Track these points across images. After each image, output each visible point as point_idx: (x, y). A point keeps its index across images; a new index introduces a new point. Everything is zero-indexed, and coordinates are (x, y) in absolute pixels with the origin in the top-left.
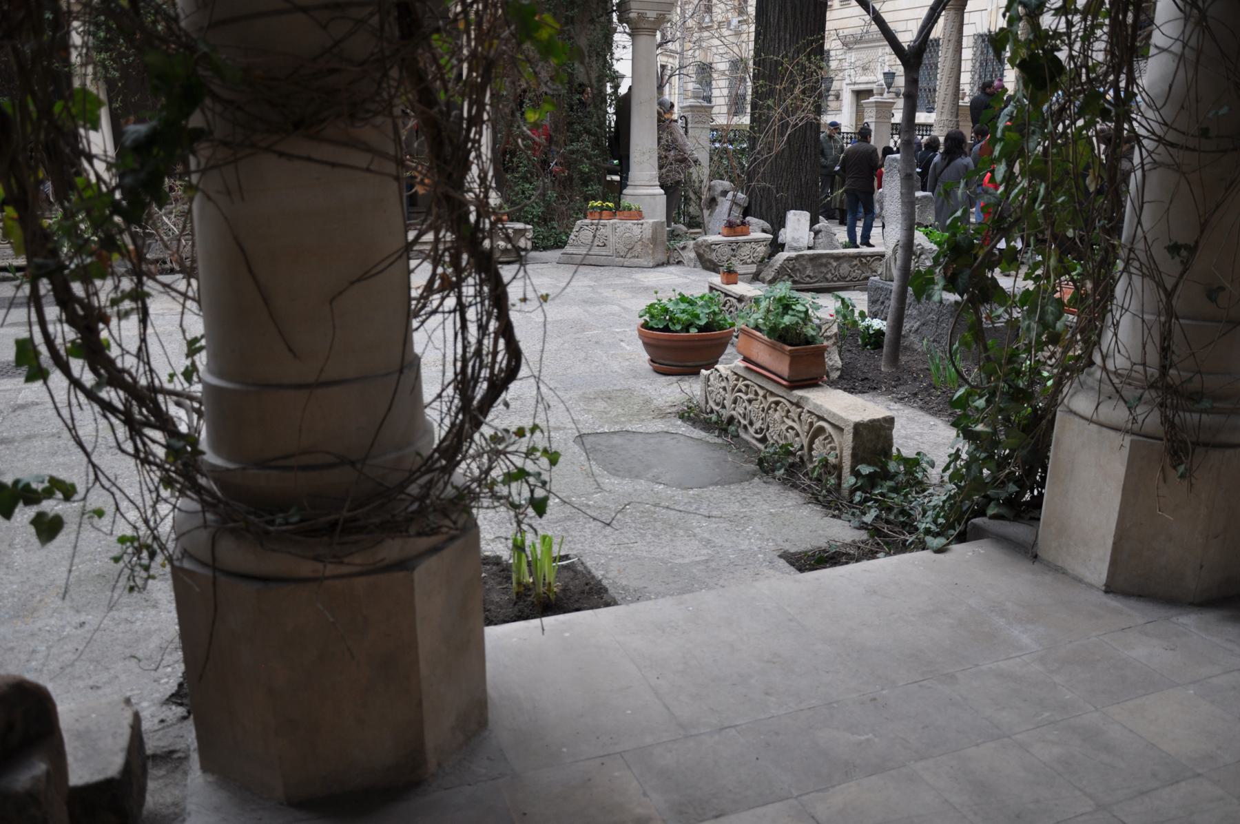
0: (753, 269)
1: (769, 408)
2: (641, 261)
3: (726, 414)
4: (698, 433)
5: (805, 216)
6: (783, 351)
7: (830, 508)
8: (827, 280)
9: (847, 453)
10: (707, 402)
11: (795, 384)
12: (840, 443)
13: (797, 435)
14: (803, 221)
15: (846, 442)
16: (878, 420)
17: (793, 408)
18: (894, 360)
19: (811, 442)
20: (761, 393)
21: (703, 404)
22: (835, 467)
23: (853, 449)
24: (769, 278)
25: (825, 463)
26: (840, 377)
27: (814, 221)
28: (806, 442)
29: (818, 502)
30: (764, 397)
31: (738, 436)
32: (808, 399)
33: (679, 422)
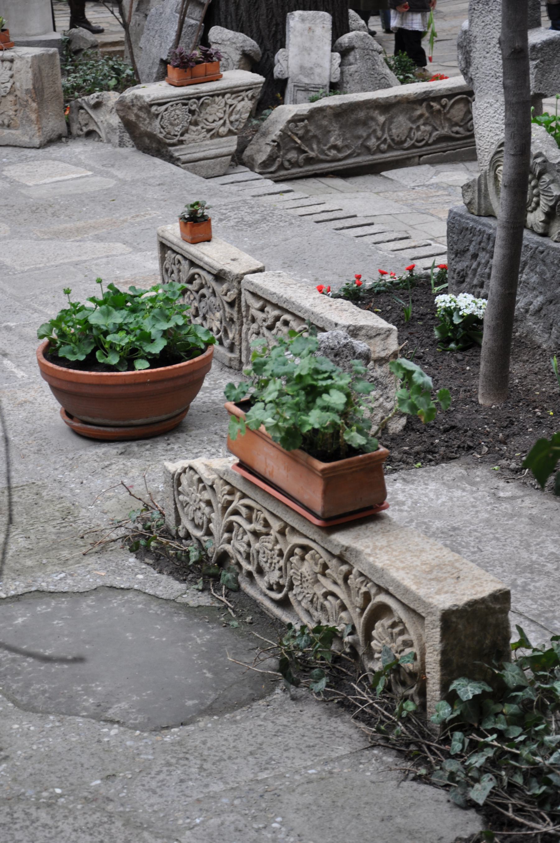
0: (231, 144)
1: (291, 554)
2: (16, 135)
3: (215, 546)
4: (169, 586)
5: (322, 21)
6: (311, 469)
7: (407, 757)
8: (369, 151)
9: (433, 661)
10: (178, 521)
11: (334, 523)
12: (420, 637)
13: (343, 607)
14: (319, 31)
15: (429, 647)
16: (483, 600)
17: (333, 563)
18: (500, 381)
19: (369, 626)
20: (276, 526)
21: (171, 520)
22: (413, 675)
23: (443, 653)
24: (261, 158)
25: (395, 668)
26: (406, 428)
27: (340, 27)
28: (359, 623)
29: (387, 744)
30: (282, 533)
31: (238, 589)
32: (357, 553)
33: (132, 560)
